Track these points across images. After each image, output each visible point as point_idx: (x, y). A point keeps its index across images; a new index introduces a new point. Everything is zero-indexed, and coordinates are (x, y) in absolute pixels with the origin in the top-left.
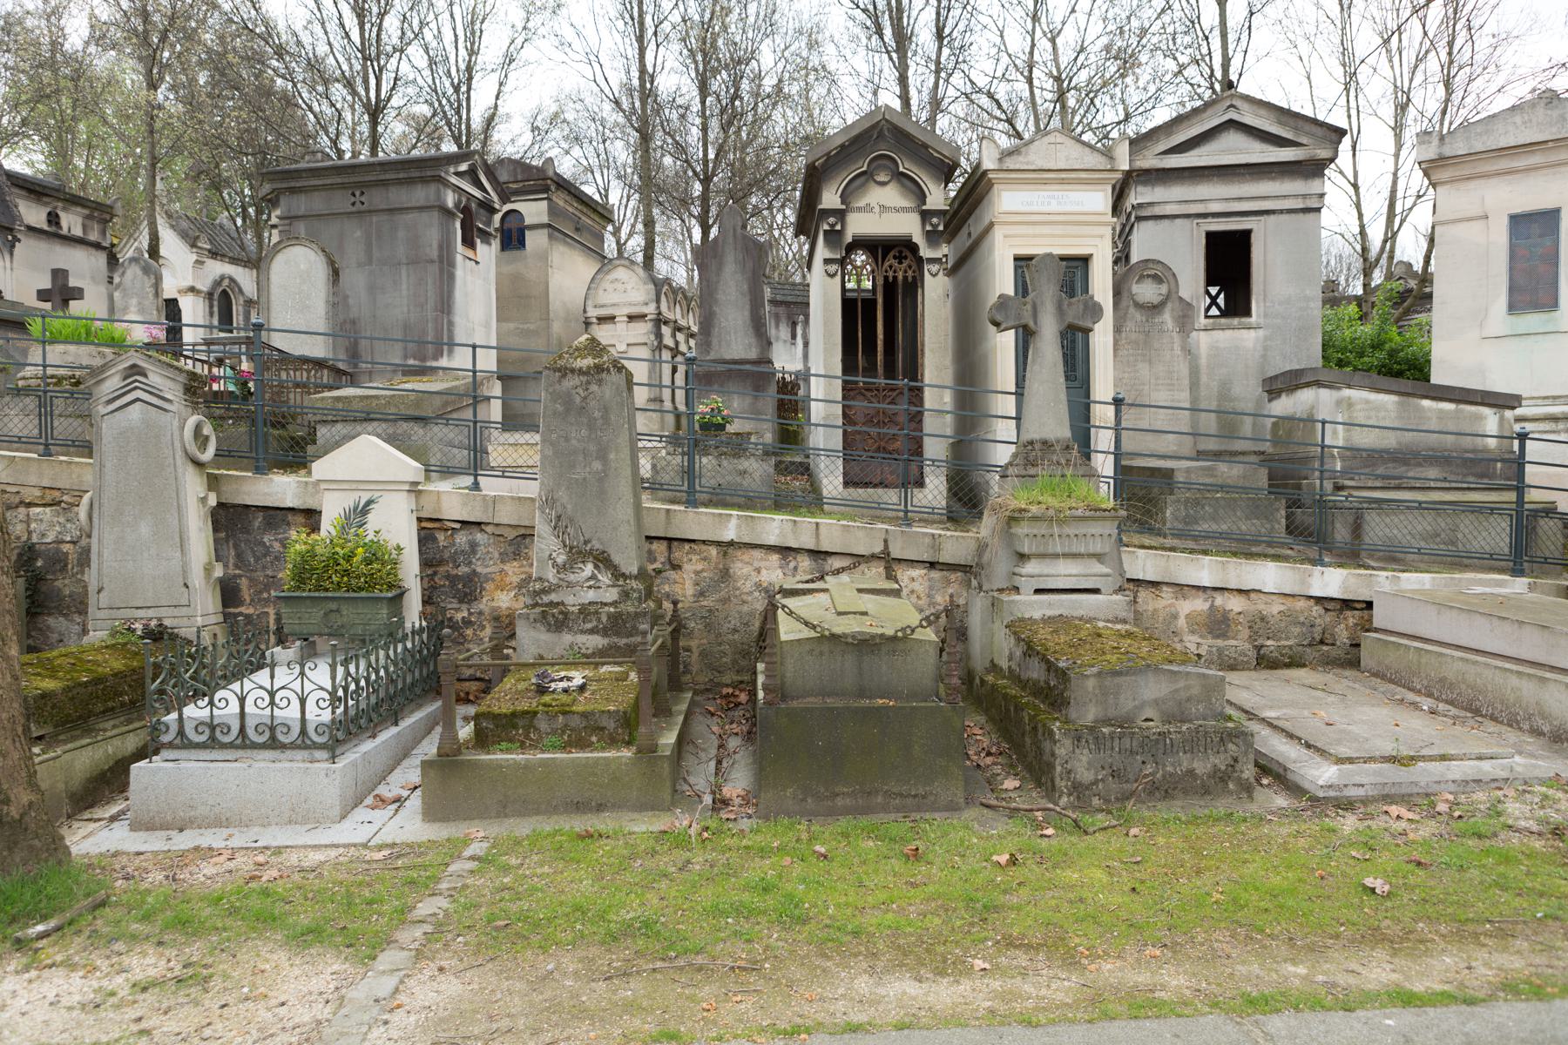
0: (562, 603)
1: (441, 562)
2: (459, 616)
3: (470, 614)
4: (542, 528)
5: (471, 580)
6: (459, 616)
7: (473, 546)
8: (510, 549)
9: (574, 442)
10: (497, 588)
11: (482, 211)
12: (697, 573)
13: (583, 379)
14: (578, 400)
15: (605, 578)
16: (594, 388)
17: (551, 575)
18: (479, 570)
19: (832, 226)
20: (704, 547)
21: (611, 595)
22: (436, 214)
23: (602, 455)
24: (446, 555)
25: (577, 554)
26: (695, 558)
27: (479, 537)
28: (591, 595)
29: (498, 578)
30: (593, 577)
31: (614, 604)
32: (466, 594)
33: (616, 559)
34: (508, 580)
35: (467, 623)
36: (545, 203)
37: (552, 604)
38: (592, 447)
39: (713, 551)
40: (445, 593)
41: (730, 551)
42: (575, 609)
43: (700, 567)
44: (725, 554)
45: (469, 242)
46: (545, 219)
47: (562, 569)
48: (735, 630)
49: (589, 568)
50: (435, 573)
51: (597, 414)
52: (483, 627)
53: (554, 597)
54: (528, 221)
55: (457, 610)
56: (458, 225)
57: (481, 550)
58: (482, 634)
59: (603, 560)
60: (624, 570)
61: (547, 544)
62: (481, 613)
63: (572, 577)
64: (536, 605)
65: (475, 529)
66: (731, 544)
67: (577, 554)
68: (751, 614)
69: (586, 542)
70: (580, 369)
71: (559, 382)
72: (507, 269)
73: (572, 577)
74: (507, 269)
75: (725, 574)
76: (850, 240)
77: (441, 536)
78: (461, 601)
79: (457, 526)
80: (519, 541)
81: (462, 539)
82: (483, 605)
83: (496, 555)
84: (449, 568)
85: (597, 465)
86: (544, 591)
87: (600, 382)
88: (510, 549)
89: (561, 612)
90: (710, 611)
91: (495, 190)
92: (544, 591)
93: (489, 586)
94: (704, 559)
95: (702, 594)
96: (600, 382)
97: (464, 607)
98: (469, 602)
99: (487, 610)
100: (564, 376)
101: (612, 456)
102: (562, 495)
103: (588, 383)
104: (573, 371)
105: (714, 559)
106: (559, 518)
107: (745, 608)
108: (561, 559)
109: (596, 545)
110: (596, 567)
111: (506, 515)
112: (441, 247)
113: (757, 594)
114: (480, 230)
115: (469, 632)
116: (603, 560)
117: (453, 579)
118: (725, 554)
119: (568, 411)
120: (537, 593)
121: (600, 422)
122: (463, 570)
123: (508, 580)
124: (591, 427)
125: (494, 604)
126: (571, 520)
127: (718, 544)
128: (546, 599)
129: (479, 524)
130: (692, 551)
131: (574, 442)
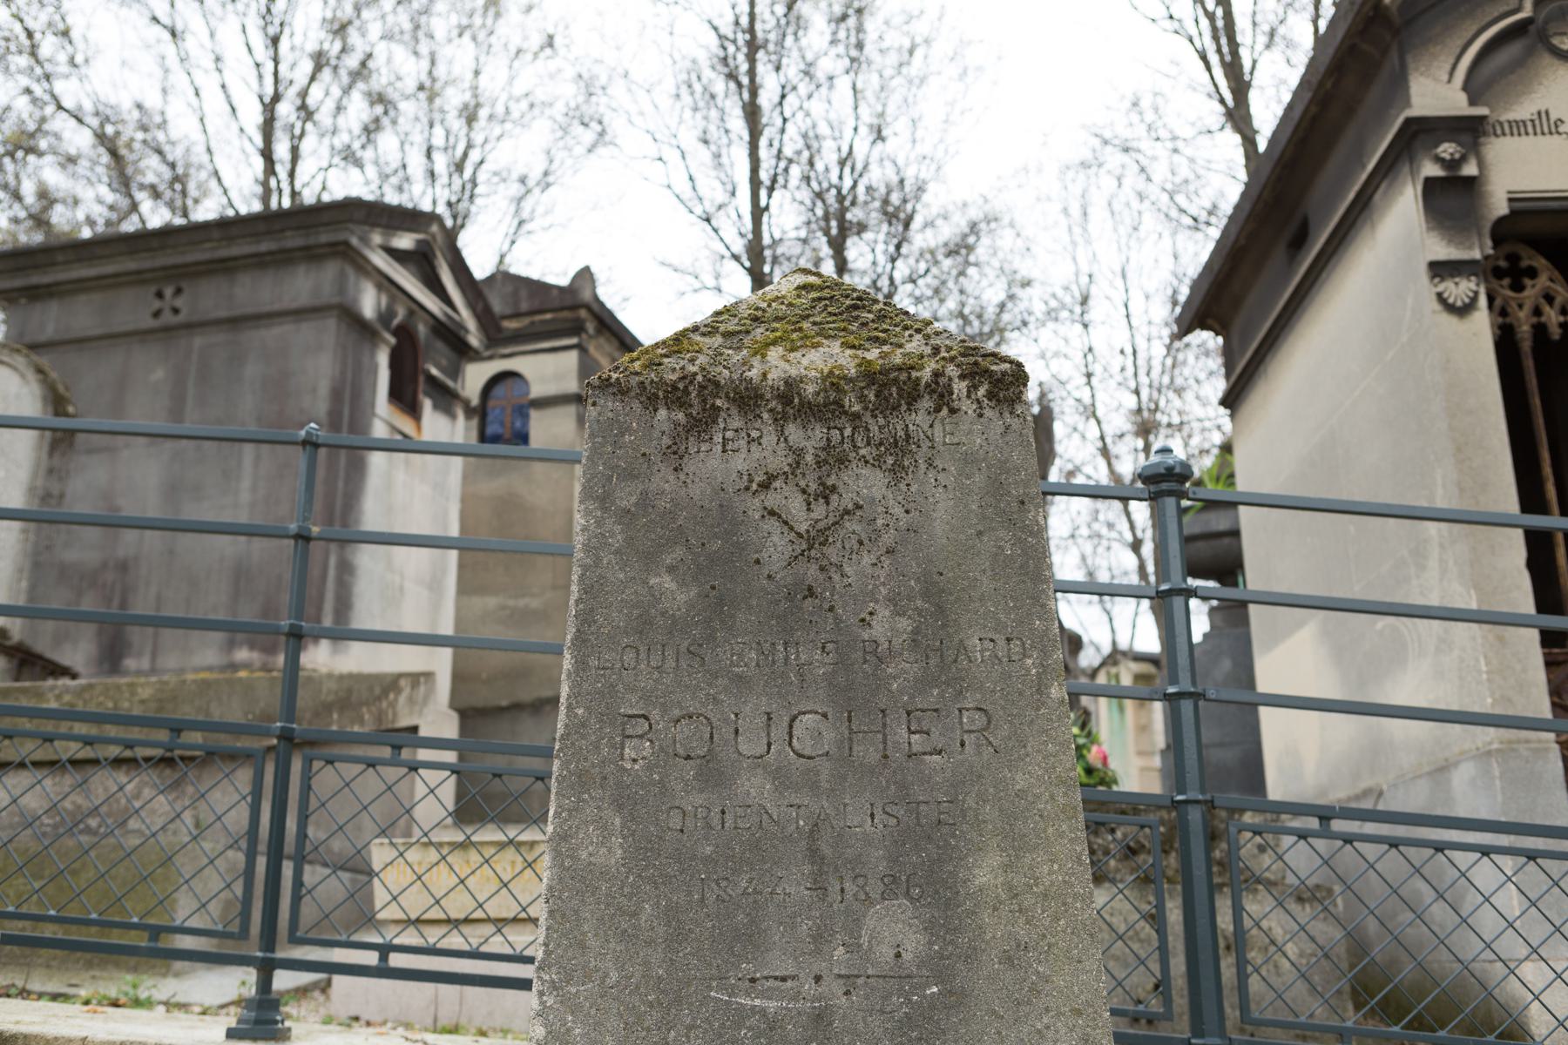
9: (755, 787)
11: (440, 345)
13: (809, 438)
14: (776, 547)
16: (864, 483)
19: (1452, 164)
22: (331, 323)
23: (925, 866)
36: (572, 358)
38: (862, 820)
45: (404, 397)
46: (572, 386)
51: (885, 626)
54: (537, 390)
56: (383, 359)
70: (789, 392)
71: (675, 455)
72: (490, 487)
74: (490, 487)
76: (1500, 207)
85: (894, 931)
87: (897, 455)
91: (471, 305)
96: (897, 455)
100: (701, 425)
101: (985, 873)
103: (833, 458)
104: (748, 398)
112: (336, 395)
114: (431, 380)
119: (718, 608)
121: (903, 670)
124: (855, 694)
131: (755, 787)
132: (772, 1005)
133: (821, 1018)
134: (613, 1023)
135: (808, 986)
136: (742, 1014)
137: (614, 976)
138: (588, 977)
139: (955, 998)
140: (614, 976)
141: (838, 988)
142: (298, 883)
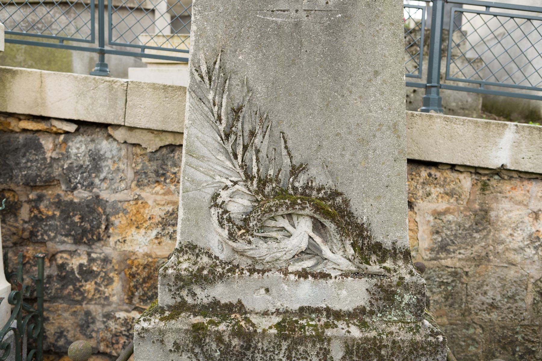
0: (240, 307)
1: (49, 182)
2: (75, 263)
3: (91, 260)
4: (200, 136)
5: (93, 211)
6: (75, 263)
7: (96, 159)
8: (152, 166)
10: (131, 223)
12: (438, 215)
15: (338, 256)
17: (215, 239)
18: (104, 195)
20: (451, 175)
21: (352, 294)
24: (57, 172)
25: (279, 195)
26: (435, 191)
27: (105, 146)
28: (305, 293)
29: (131, 208)
30: (311, 251)
31: (358, 315)
32: (85, 232)
33: (363, 210)
34: (147, 212)
35: (86, 273)
37: (216, 309)
39: (466, 182)
40: (55, 228)
41: (494, 182)
42: (266, 324)
43: (442, 206)
44: (485, 187)
47: (241, 228)
48: (493, 306)
49: (302, 231)
50: (40, 198)
52: (110, 281)
53: (221, 292)
55: (72, 253)
57: (108, 166)
58: (108, 291)
59: (333, 213)
60: (379, 237)
61: (208, 168)
62: (106, 260)
63: (262, 250)
64: (178, 309)
65: (99, 134)
66: (501, 172)
67: (279, 195)
68: (521, 283)
69: (295, 171)
73: (262, 250)
75: (482, 219)
77: (47, 143)
78: (78, 241)
79: (72, 128)
80: (163, 156)
81: (79, 148)
82: (110, 248)
83: (130, 174)
84: (61, 190)
86: (199, 278)
88: (152, 166)
89: (238, 332)
90: (455, 274)
92: (199, 278)
93: (118, 220)
94: (450, 194)
95: (443, 248)
97: (82, 249)
98: (90, 243)
99: (115, 256)
102: (246, 63)
105: (466, 196)
106: (236, 112)
107: (512, 274)
108: (239, 205)
109: (319, 177)
110: (318, 227)
111: (144, 114)
113: (530, 252)
115: (89, 286)
116: (333, 213)
117: (67, 208)
118: (485, 187)
120: (182, 282)
122: (81, 195)
123: (147, 212)
125: (127, 248)
126: (264, 119)
127: (476, 170)
128: (203, 295)
129: (104, 126)
130: (432, 180)
132: (279, 20)
133: (297, 25)
134: (221, 25)
135: (293, 13)
136: (268, 23)
137: (221, 9)
138: (212, 9)
139: (347, 18)
140: (221, 9)
141: (304, 14)
142: (111, 24)
